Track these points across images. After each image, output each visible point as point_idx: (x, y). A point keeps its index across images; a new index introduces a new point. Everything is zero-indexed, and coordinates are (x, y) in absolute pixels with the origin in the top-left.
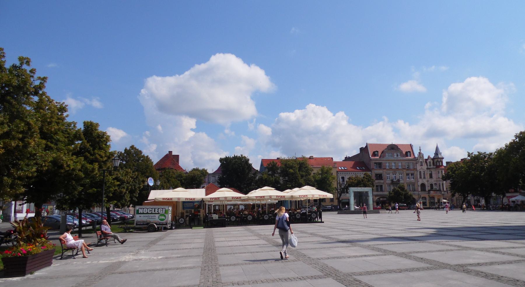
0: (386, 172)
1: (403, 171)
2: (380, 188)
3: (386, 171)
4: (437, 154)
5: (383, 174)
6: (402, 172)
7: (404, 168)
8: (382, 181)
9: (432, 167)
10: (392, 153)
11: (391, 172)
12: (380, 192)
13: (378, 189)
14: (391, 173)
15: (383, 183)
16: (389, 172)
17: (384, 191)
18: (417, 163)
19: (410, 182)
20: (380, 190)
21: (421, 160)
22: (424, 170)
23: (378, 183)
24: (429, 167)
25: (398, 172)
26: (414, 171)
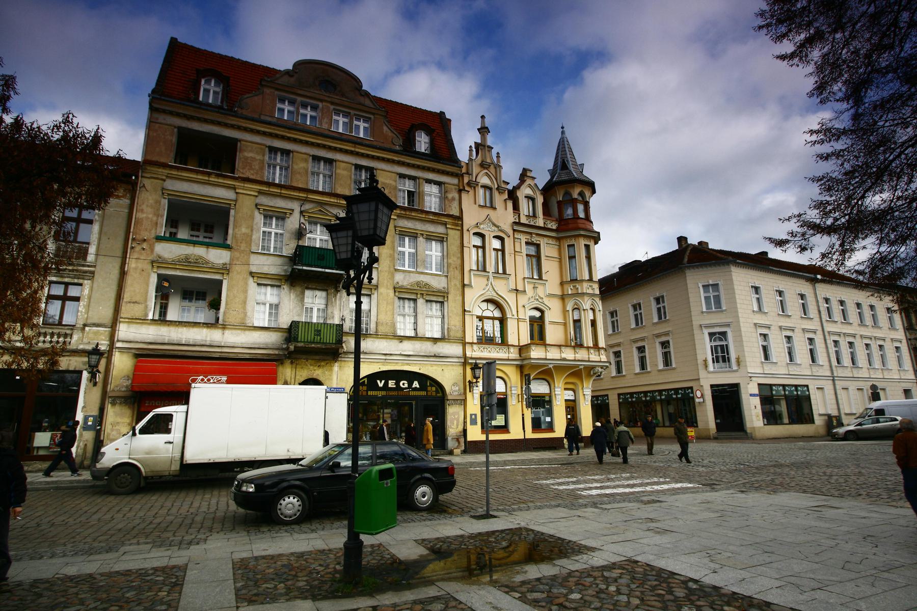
0: (264, 200)
3: (260, 192)
4: (564, 166)
5: (232, 212)
8: (217, 256)
9: (540, 222)
10: (321, 105)
11: (296, 206)
14: (296, 214)
15: (225, 269)
16: (280, 203)
18: (460, 191)
19: (418, 284)
23: (186, 262)
24: (524, 220)
26: (445, 224)
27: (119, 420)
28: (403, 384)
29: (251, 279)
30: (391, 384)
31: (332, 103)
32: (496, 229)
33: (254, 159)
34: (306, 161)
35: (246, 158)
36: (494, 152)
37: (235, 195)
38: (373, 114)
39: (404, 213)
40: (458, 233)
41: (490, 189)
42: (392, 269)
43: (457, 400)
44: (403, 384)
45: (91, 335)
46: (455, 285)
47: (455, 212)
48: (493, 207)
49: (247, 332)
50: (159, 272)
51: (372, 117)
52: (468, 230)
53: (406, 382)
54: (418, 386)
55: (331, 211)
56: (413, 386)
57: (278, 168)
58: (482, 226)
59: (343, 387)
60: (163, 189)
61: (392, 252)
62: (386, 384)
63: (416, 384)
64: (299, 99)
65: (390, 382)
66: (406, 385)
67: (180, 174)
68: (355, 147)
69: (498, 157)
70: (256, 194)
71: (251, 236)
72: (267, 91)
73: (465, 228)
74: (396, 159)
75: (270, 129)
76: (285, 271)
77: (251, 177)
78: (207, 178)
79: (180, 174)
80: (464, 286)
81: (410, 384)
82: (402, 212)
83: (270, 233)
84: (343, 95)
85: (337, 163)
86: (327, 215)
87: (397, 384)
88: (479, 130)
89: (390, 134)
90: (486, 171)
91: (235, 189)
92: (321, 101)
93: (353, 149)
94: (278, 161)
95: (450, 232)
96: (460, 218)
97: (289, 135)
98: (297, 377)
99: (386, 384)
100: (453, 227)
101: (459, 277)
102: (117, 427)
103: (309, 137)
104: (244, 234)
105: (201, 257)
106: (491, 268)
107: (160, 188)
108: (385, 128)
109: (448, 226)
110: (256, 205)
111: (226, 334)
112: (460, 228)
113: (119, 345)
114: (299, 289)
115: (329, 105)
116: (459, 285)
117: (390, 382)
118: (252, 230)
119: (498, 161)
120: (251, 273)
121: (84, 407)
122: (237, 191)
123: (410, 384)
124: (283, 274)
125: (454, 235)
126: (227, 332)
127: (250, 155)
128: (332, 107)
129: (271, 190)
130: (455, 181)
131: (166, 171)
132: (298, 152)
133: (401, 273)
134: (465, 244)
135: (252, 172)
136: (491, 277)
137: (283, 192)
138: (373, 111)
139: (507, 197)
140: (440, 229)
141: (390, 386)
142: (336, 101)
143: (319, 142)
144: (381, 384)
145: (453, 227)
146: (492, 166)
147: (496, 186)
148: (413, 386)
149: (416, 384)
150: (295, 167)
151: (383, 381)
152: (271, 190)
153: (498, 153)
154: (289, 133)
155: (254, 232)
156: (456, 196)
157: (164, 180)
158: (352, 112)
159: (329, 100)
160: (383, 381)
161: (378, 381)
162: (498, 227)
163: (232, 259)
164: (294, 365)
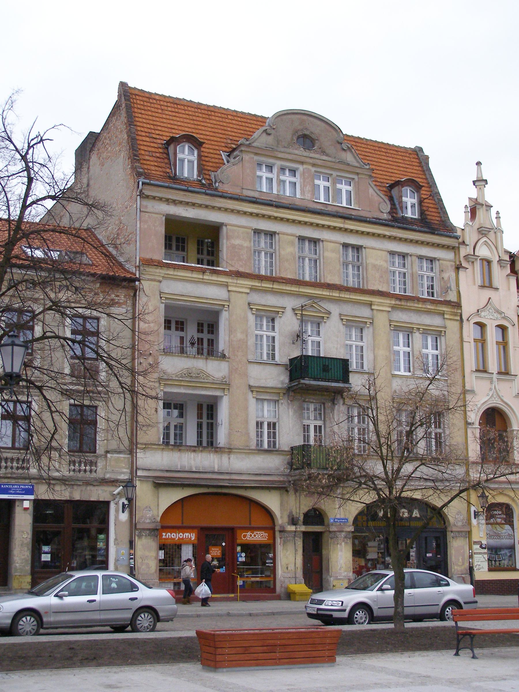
1: (370, 304)
2: (200, 426)
3: (253, 289)
6: (365, 312)
7: (383, 288)
10: (301, 168)
12: (193, 449)
13: (180, 427)
14: (289, 313)
16: (271, 300)
17: (229, 450)
18: (458, 268)
20: (200, 443)
21: (483, 252)
22: (505, 318)
25: (335, 309)
26: (442, 314)
27: (147, 553)
28: (403, 513)
29: (250, 393)
31: (314, 165)
32: (499, 316)
33: (241, 247)
34: (292, 243)
35: (234, 246)
36: (493, 211)
37: (227, 293)
38: (358, 174)
39: (400, 303)
40: (457, 324)
41: (489, 262)
42: (389, 375)
43: (461, 532)
45: (113, 463)
47: (452, 297)
48: (490, 286)
49: (251, 457)
50: (165, 390)
51: (356, 177)
52: (468, 320)
53: (406, 511)
54: (418, 516)
55: (323, 305)
56: (414, 516)
57: (263, 253)
58: (483, 314)
59: (346, 517)
60: (161, 293)
61: (388, 354)
64: (279, 163)
66: (406, 515)
67: (176, 273)
68: (344, 223)
69: (498, 218)
70: (248, 291)
71: (247, 342)
72: (246, 157)
73: (465, 317)
74: (387, 233)
75: (258, 209)
76: (282, 383)
77: (241, 270)
78: (201, 277)
79: (176, 273)
81: (410, 512)
82: (398, 302)
83: (262, 336)
84: (324, 152)
85: (324, 243)
86: (320, 312)
88: (474, 182)
89: (376, 198)
90: (485, 239)
91: (227, 286)
92: (302, 163)
93: (342, 225)
94: (263, 245)
95: (449, 323)
96: (458, 305)
97: (276, 215)
98: (302, 507)
100: (452, 317)
102: (146, 561)
103: (297, 215)
104: (240, 340)
105: (202, 371)
106: (493, 366)
107: (158, 293)
108: (371, 191)
109: (446, 316)
110: (249, 304)
111: (231, 458)
112: (459, 318)
113: (139, 473)
114: (296, 404)
115: (310, 167)
118: (247, 336)
119: (499, 223)
120: (250, 387)
121: (116, 539)
122: (230, 288)
123: (410, 512)
124: (280, 386)
125: (452, 326)
126: (232, 456)
127: (237, 242)
128: (313, 169)
129: (263, 285)
130: (449, 255)
131: (163, 271)
132: (284, 234)
134: (465, 338)
135: (241, 263)
136: (495, 379)
137: (275, 286)
138: (358, 171)
139: (509, 272)
140: (436, 321)
142: (319, 162)
143: (306, 220)
145: (452, 317)
146: (492, 233)
147: (497, 259)
148: (414, 516)
149: (416, 513)
150: (283, 253)
152: (263, 285)
153: (498, 213)
154: (276, 212)
155: (249, 338)
156: (453, 275)
157: (160, 282)
158: (335, 174)
159: (311, 161)
162: (500, 313)
163: (231, 372)
164: (298, 494)
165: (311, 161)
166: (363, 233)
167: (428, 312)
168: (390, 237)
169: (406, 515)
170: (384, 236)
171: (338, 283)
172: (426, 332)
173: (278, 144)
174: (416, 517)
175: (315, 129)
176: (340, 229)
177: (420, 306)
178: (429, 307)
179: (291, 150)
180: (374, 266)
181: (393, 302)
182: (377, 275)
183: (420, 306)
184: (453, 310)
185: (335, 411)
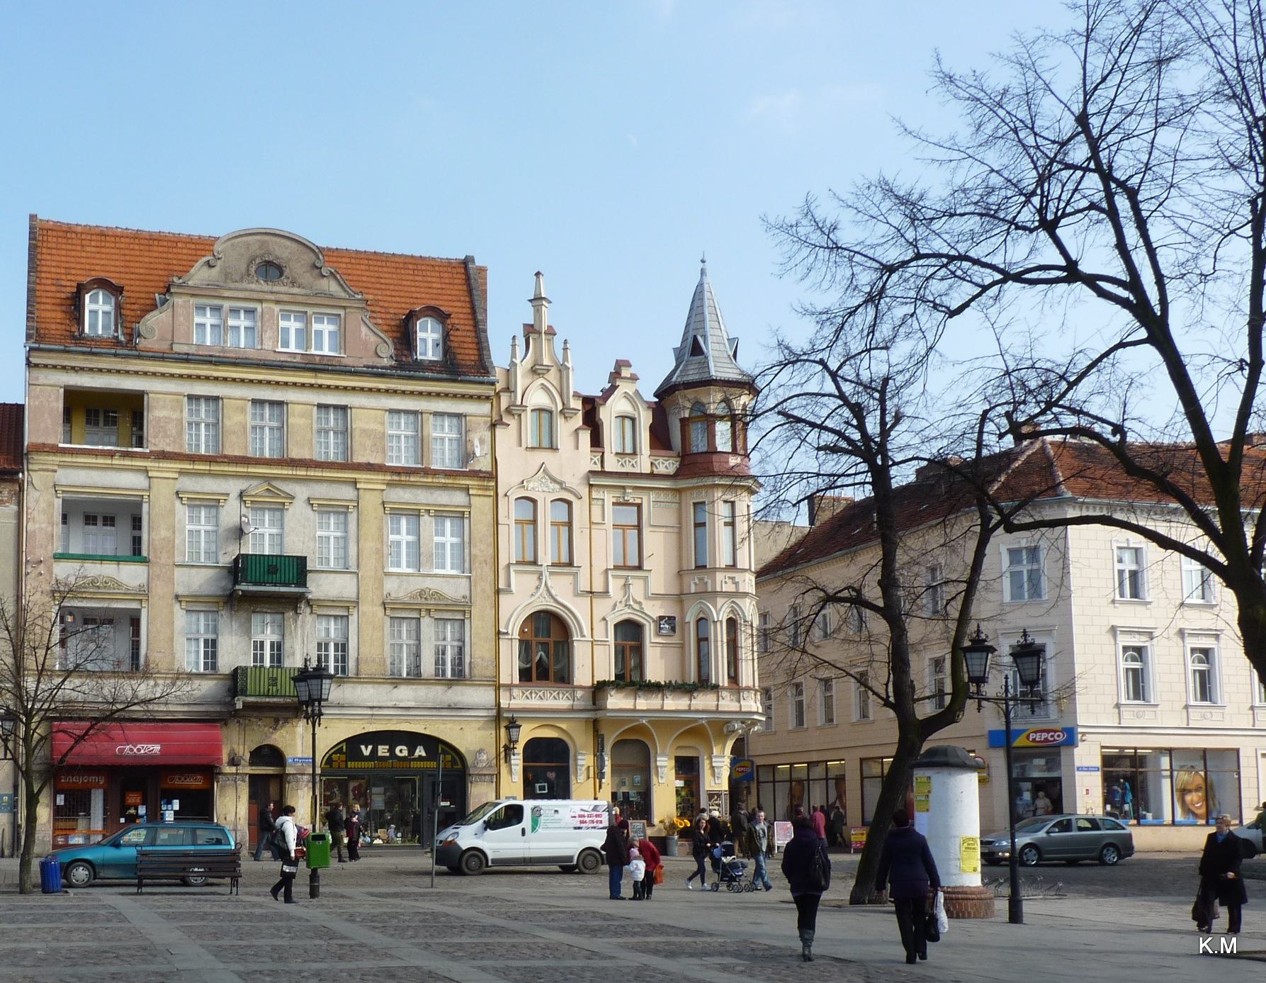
19: (422, 593)
28: (401, 751)
30: (383, 750)
31: (278, 302)
34: (243, 410)
44: (401, 751)
46: (484, 591)
53: (404, 748)
62: (374, 751)
63: (420, 751)
64: (227, 305)
65: (380, 747)
66: (405, 753)
74: (382, 386)
80: (498, 592)
81: (411, 752)
82: (395, 478)
87: (392, 750)
99: (374, 751)
100: (480, 492)
101: (491, 577)
116: (490, 591)
117: (380, 747)
125: (481, 505)
133: (394, 578)
141: (380, 754)
142: (285, 298)
144: (366, 751)
149: (420, 751)
151: (370, 747)
159: (272, 297)
160: (370, 747)
161: (363, 747)
165: (272, 297)
166: (345, 388)
167: (445, 487)
168: (387, 391)
169: (405, 753)
170: (379, 390)
171: (308, 457)
172: (440, 514)
173: (226, 278)
174: (420, 756)
175: (281, 251)
176: (312, 386)
177: (430, 480)
178: (443, 481)
179: (245, 285)
180: (364, 431)
181: (388, 478)
182: (368, 443)
183: (430, 480)
184: (480, 483)
185: (299, 623)
